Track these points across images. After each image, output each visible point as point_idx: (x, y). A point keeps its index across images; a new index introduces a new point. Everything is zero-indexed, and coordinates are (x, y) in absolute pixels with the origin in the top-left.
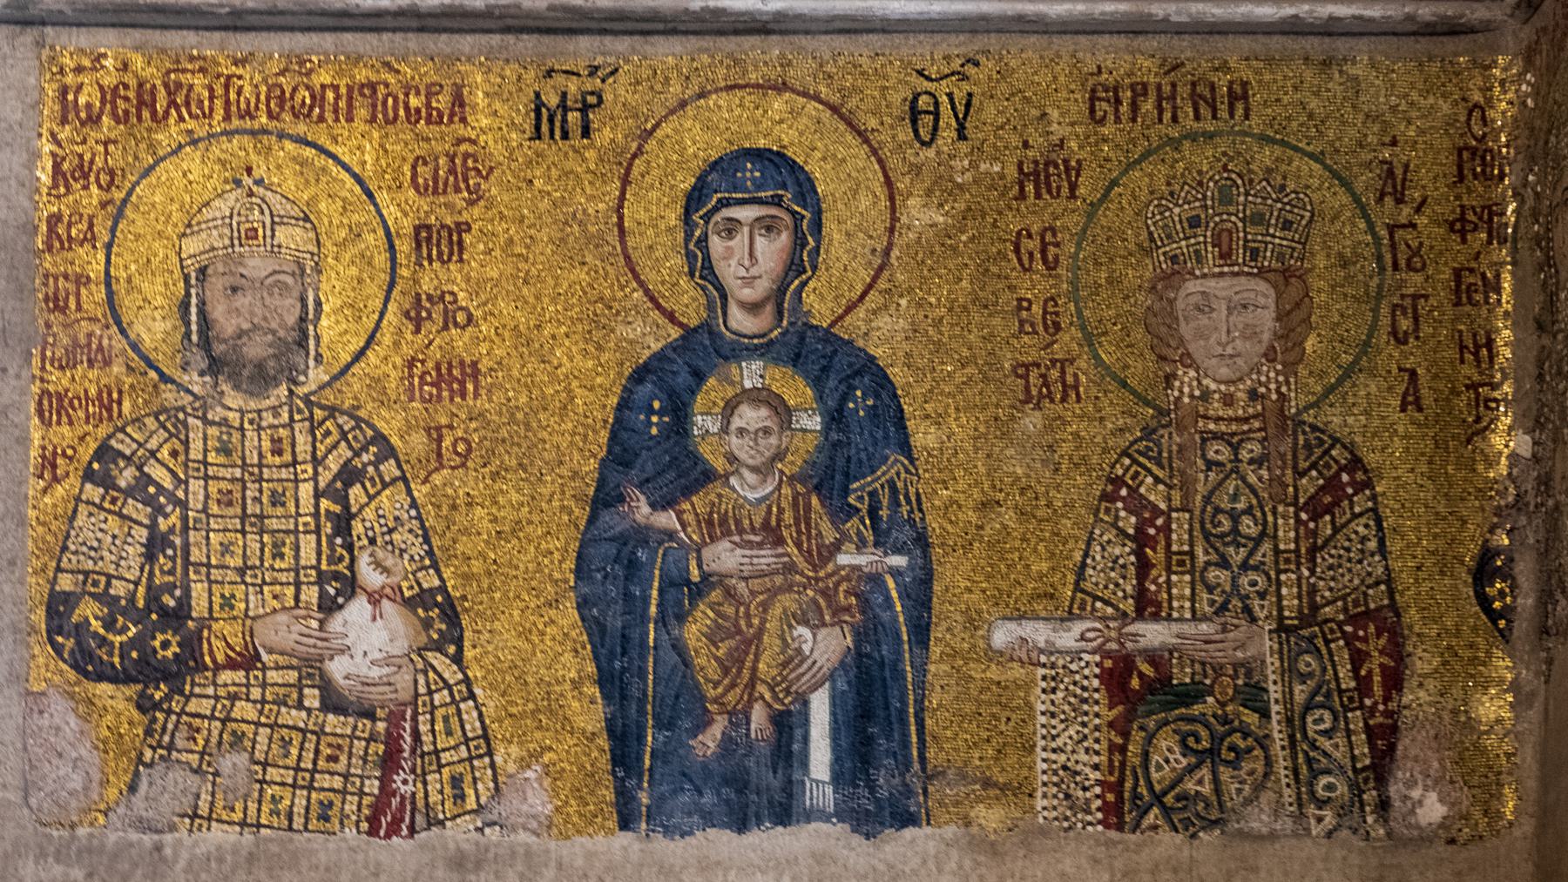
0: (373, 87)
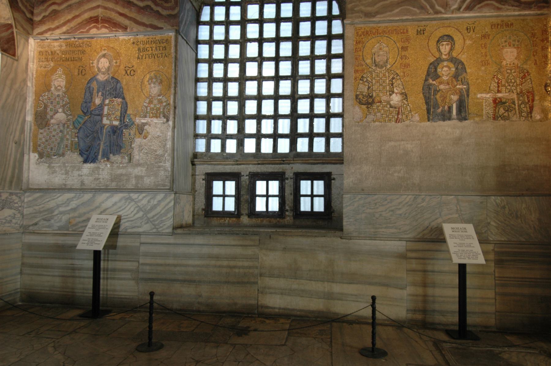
0: (396, 29)
